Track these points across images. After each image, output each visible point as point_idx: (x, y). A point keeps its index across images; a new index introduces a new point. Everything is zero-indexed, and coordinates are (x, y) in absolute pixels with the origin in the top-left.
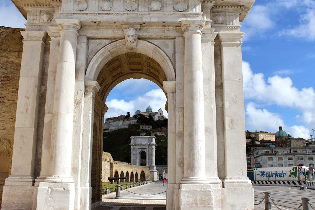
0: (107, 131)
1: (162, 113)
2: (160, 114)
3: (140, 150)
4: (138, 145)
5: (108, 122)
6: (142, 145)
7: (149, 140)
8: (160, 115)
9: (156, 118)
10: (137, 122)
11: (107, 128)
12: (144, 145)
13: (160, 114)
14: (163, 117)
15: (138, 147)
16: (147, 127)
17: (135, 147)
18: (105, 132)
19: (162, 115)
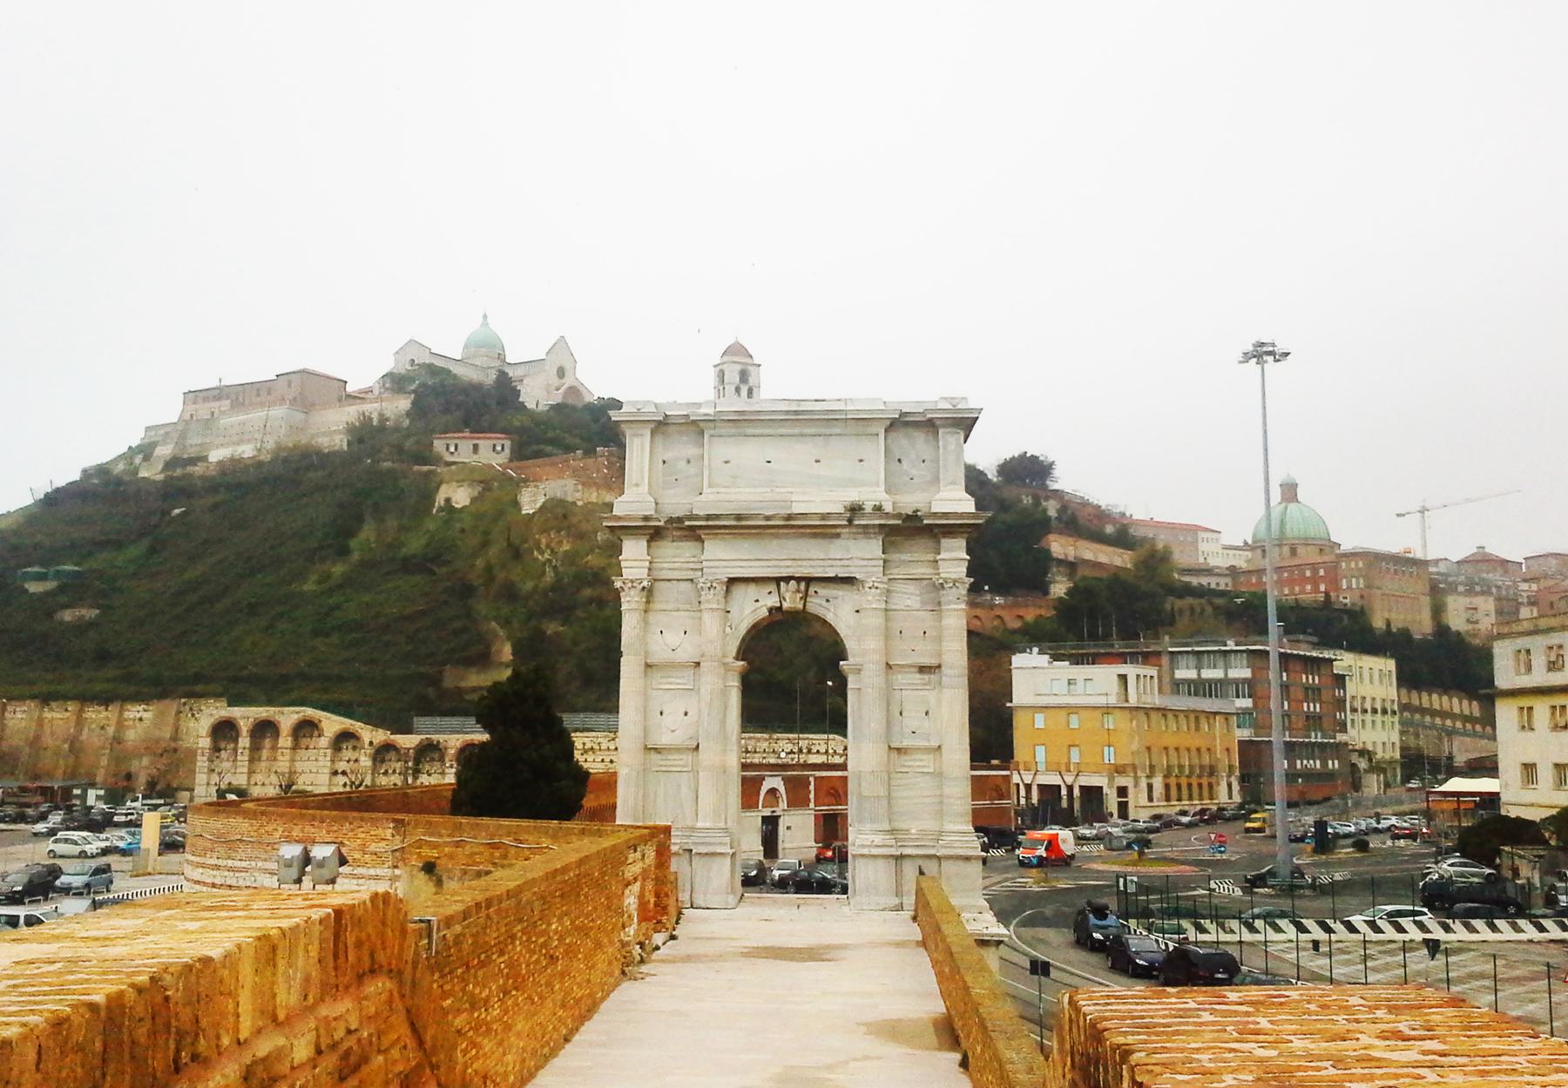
0: (198, 469)
1: (568, 366)
2: (561, 373)
3: (752, 607)
4: (741, 526)
5: (203, 411)
6: (792, 526)
7: (893, 459)
8: (556, 381)
9: (536, 395)
10: (408, 414)
11: (192, 452)
12: (821, 530)
13: (561, 373)
14: (574, 391)
15: (724, 557)
16: (485, 444)
17: (675, 555)
18: (179, 472)
19: (568, 382)
